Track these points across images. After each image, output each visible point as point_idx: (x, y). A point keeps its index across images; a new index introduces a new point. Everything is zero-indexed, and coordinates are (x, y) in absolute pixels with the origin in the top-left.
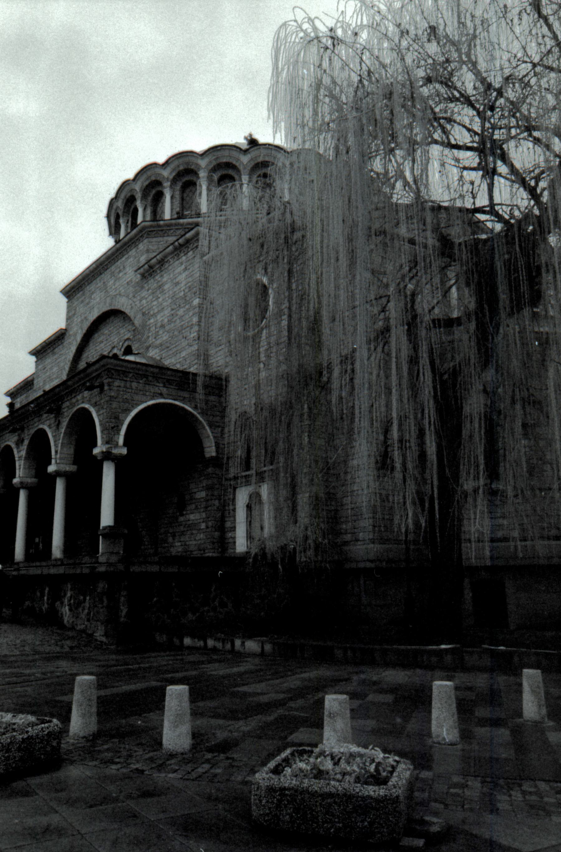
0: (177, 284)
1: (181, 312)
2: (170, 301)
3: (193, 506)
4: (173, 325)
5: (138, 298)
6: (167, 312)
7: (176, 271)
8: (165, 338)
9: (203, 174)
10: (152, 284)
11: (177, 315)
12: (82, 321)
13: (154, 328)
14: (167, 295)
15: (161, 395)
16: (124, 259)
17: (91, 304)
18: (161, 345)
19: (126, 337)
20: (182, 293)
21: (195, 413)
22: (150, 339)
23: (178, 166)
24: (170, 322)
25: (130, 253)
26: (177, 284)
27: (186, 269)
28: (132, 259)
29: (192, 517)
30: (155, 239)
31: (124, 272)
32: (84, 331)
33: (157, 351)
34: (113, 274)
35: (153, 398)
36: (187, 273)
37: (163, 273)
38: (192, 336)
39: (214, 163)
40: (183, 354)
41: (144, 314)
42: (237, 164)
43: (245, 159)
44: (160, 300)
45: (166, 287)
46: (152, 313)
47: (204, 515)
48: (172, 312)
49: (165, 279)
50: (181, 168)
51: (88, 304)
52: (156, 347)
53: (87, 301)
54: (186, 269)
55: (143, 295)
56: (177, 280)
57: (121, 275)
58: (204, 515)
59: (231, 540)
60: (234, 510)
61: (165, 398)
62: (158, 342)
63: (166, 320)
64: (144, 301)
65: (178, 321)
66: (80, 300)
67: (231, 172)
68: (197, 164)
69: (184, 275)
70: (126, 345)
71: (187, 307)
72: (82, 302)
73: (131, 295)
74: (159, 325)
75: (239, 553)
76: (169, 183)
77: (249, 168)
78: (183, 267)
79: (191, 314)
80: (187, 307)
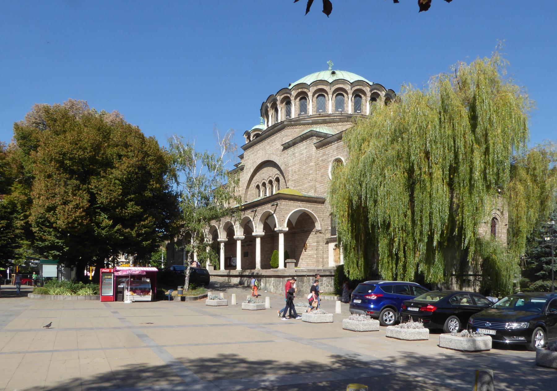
0: (302, 154)
1: (304, 167)
2: (298, 161)
3: (311, 248)
4: (300, 172)
5: (283, 157)
6: (297, 166)
7: (301, 149)
8: (297, 177)
9: (310, 94)
10: (290, 151)
11: (302, 168)
12: (253, 163)
13: (291, 172)
14: (297, 158)
15: (300, 207)
16: (274, 137)
17: (258, 156)
18: (295, 180)
19: (276, 173)
20: (305, 159)
21: (313, 213)
22: (289, 177)
24: (299, 171)
25: (277, 135)
26: (302, 154)
27: (306, 148)
28: (278, 138)
29: (310, 252)
30: (289, 130)
31: (275, 143)
32: (255, 168)
33: (293, 182)
34: (268, 143)
35: (297, 208)
37: (295, 148)
38: (310, 179)
40: (306, 186)
41: (286, 165)
44: (294, 160)
45: (296, 155)
46: (290, 165)
47: (315, 252)
48: (300, 167)
49: (296, 151)
51: (256, 155)
52: (292, 181)
53: (255, 154)
55: (285, 156)
57: (273, 144)
58: (315, 252)
59: (327, 262)
60: (328, 251)
61: (301, 207)
62: (294, 179)
63: (297, 170)
64: (286, 159)
65: (303, 171)
66: (252, 152)
69: (305, 151)
70: (276, 176)
71: (307, 165)
72: (253, 153)
73: (279, 155)
74: (294, 171)
75: (331, 267)
76: (294, 98)
78: (305, 147)
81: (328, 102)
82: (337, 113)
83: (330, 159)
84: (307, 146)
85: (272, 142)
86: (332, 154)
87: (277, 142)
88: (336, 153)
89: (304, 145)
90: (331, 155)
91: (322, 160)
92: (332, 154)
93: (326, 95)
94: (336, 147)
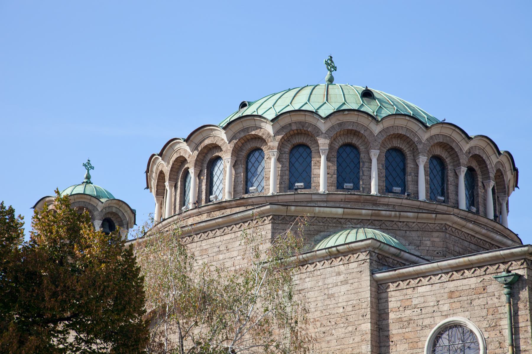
0: (330, 296)
1: (339, 332)
16: (226, 237)
23: (290, 124)
36: (347, 287)
37: (304, 276)
39: (338, 130)
42: (366, 134)
43: (376, 129)
48: (323, 329)
50: (294, 127)
54: (345, 282)
56: (330, 292)
65: (333, 343)
67: (355, 141)
68: (316, 128)
71: (350, 329)
77: (380, 141)
78: (342, 278)
79: (357, 339)
80: (350, 329)
81: (367, 165)
82: (390, 195)
83: (427, 322)
84: (350, 277)
85: (216, 249)
86: (435, 308)
87: (235, 254)
88: (446, 308)
89: (339, 274)
90: (431, 310)
91: (400, 320)
92: (435, 308)
93: (362, 148)
94: (447, 290)
